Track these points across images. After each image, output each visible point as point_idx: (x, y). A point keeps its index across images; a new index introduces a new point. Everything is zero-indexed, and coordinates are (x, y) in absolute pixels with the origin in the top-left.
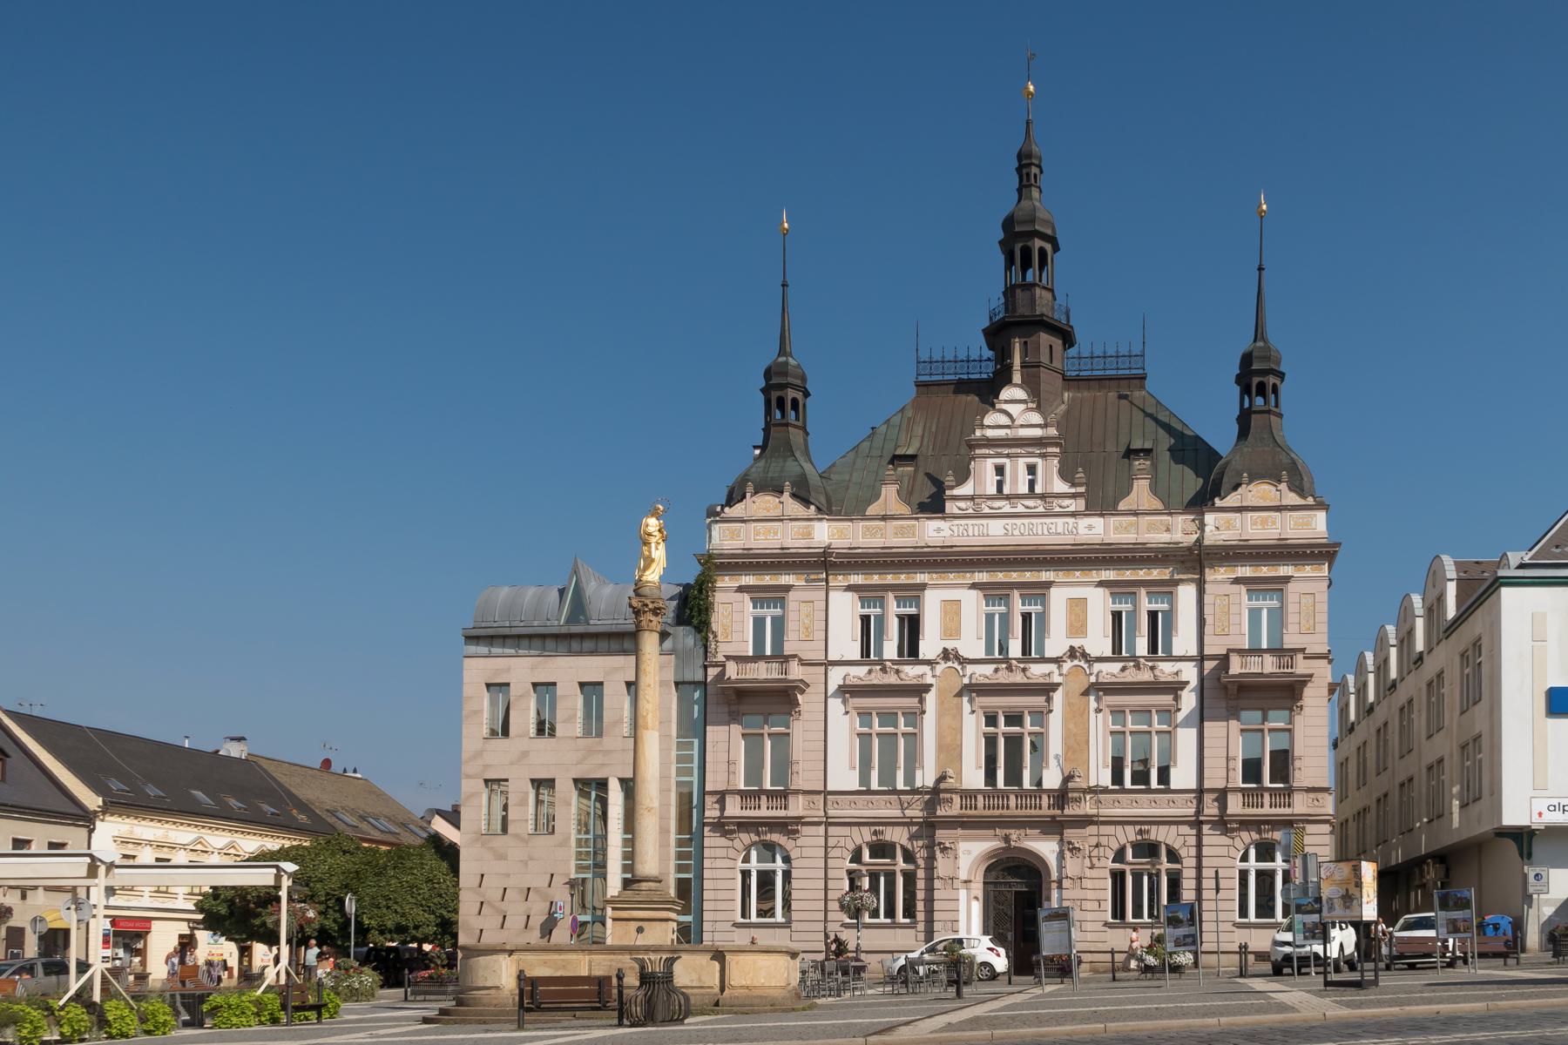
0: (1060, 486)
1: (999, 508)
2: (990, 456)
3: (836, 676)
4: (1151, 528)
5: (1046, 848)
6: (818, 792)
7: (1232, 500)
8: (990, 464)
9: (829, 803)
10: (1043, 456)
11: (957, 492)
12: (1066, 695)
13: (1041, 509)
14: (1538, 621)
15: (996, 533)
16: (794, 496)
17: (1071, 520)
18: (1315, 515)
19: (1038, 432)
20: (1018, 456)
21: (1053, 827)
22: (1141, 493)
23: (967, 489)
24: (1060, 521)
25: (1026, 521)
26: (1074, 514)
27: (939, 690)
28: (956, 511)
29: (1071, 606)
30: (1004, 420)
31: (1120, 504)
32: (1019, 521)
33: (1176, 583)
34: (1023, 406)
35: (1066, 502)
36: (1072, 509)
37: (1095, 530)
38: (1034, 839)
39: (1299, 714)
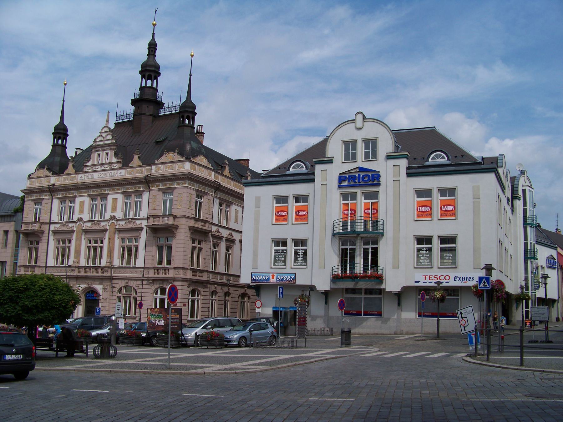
0: (114, 160)
1: (98, 169)
2: (97, 151)
3: (52, 228)
4: (137, 172)
5: (99, 288)
6: (43, 267)
7: (161, 160)
8: (97, 153)
9: (47, 270)
10: (110, 149)
11: (87, 164)
12: (109, 232)
13: (108, 168)
14: (258, 199)
15: (96, 177)
16: (47, 169)
17: (115, 171)
18: (185, 164)
19: (110, 142)
20: (104, 150)
21: (101, 279)
22: (136, 160)
23: (90, 163)
24: (113, 172)
25: (104, 172)
26: (117, 169)
27: (77, 232)
28: (87, 171)
29: (113, 201)
30: (102, 139)
31: (130, 164)
32: (102, 173)
33: (143, 191)
34: (106, 134)
35: (115, 165)
36: (117, 167)
37: (123, 174)
38: (96, 284)
39: (175, 239)
